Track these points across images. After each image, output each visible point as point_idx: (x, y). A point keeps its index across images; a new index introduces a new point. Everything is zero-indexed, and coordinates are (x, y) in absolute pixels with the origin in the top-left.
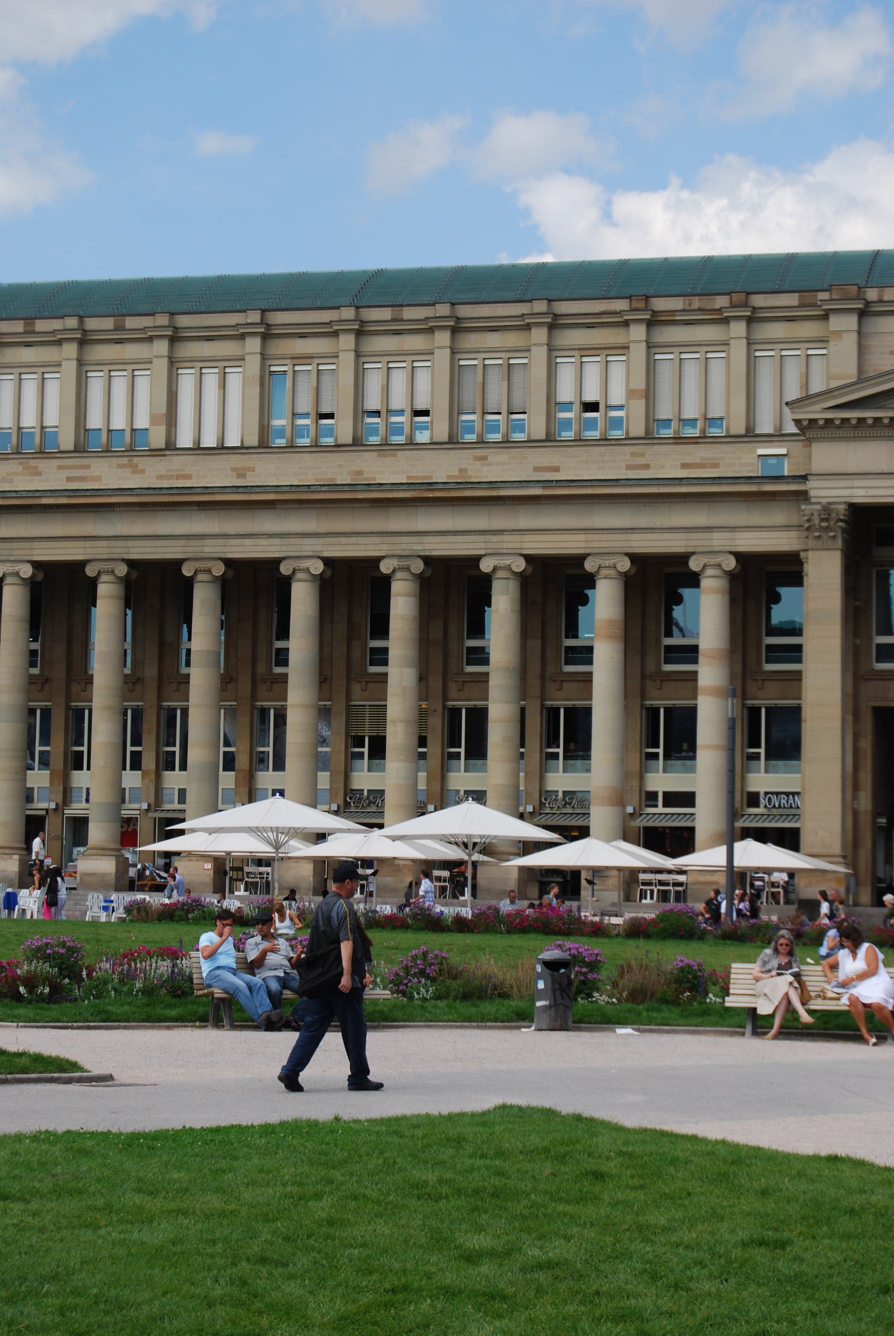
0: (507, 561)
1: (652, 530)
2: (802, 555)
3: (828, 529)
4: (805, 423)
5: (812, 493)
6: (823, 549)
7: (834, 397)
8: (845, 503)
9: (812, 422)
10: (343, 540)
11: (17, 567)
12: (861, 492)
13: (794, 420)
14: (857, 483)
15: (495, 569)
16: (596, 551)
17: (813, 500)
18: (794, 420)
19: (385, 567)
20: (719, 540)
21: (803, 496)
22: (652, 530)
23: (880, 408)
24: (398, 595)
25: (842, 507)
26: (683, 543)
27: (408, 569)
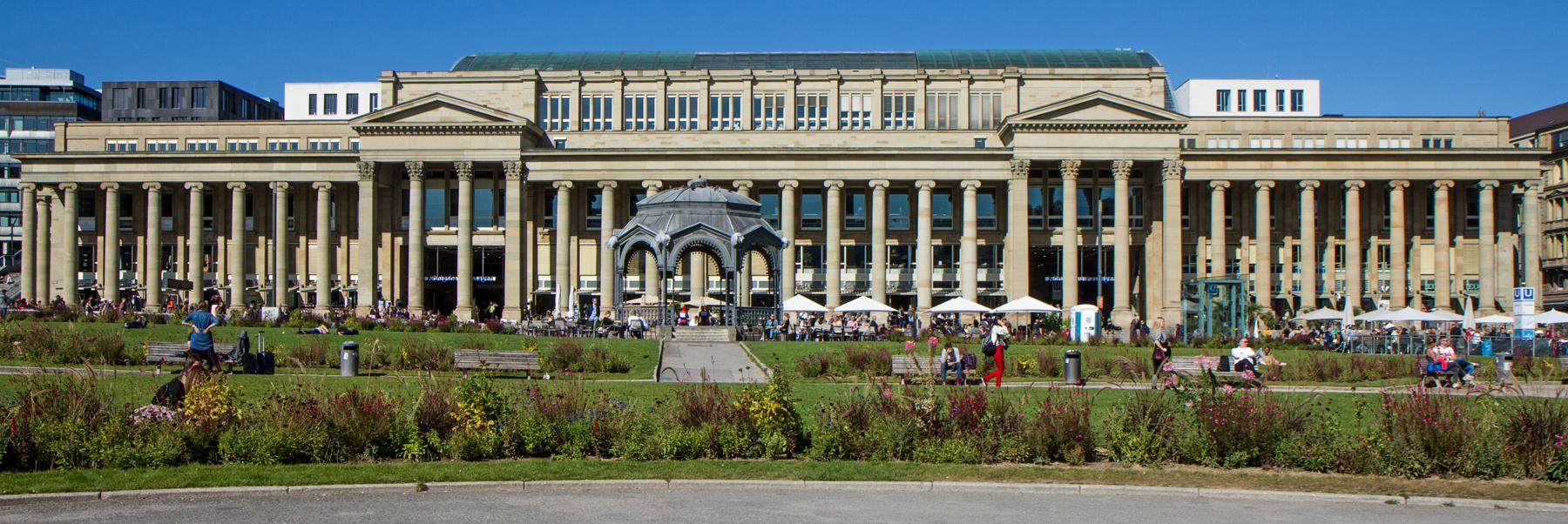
0: (880, 182)
2: (1009, 181)
3: (1022, 171)
5: (1015, 155)
10: (807, 172)
11: (655, 182)
12: (1036, 155)
14: (1034, 151)
15: (876, 185)
19: (826, 184)
20: (973, 175)
24: (831, 196)
27: (837, 185)
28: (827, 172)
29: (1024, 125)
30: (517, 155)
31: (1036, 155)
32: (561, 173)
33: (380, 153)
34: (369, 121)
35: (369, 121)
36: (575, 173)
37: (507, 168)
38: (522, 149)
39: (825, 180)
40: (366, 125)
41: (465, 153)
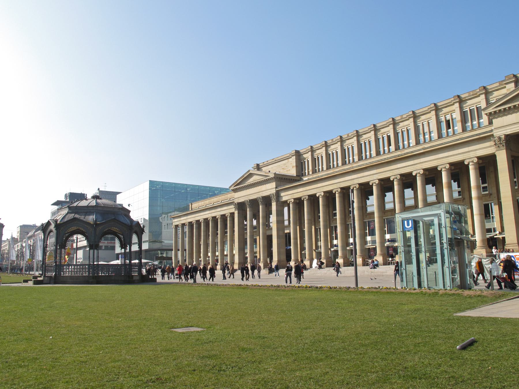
1: (454, 155)
4: (488, 114)
5: (494, 134)
6: (500, 150)
7: (495, 104)
8: (504, 135)
9: (490, 113)
12: (509, 130)
13: (485, 114)
16: (440, 164)
17: (495, 136)
18: (485, 114)
21: (492, 135)
22: (454, 155)
23: (509, 103)
25: (503, 136)
26: (462, 157)
28: (391, 171)
29: (495, 112)
30: (274, 191)
31: (509, 130)
32: (290, 196)
33: (239, 199)
34: (234, 186)
35: (234, 186)
36: (294, 195)
37: (272, 197)
38: (276, 188)
39: (465, 159)
40: (233, 188)
41: (260, 193)
